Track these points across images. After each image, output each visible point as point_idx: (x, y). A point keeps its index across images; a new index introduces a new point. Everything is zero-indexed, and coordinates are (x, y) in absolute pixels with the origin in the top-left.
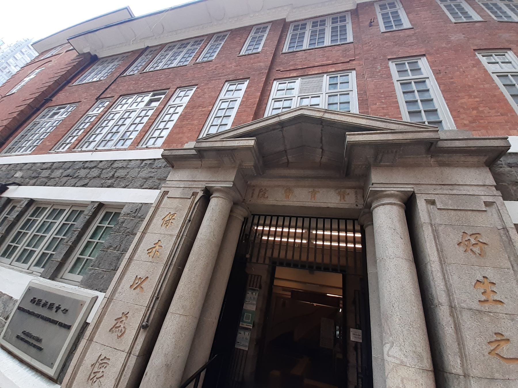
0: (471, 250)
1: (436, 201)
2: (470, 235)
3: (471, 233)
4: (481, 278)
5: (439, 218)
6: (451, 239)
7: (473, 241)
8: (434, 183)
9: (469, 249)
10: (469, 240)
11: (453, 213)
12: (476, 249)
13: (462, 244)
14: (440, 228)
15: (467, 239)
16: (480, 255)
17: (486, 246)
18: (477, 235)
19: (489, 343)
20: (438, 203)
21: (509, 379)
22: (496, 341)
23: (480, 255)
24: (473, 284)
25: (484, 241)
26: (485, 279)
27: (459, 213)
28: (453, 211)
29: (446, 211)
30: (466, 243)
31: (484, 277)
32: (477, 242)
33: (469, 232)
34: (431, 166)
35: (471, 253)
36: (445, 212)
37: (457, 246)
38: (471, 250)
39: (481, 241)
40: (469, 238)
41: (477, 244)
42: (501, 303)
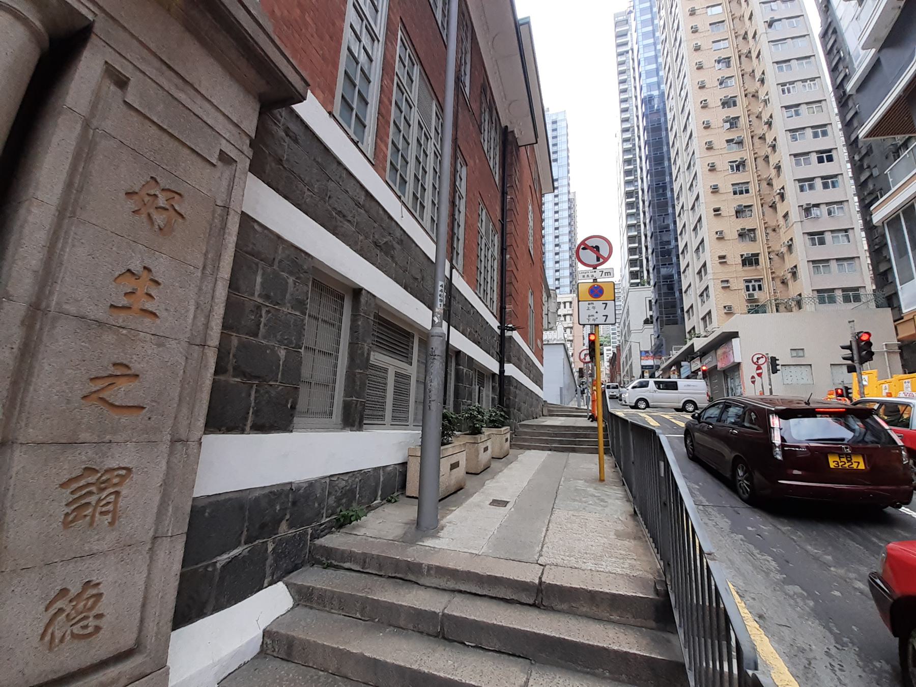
0: (149, 215)
1: (132, 83)
2: (163, 190)
3: (167, 187)
4: (136, 266)
5: (114, 121)
6: (113, 177)
7: (162, 202)
8: (152, 46)
9: (144, 211)
10: (155, 195)
11: (153, 130)
12: (160, 219)
13: (136, 197)
14: (104, 145)
15: (152, 192)
16: (161, 229)
17: (180, 220)
18: (177, 197)
19: (92, 379)
20: (131, 88)
21: (110, 441)
22: (110, 376)
23: (161, 229)
24: (117, 274)
25: (182, 212)
26: (146, 272)
27: (166, 138)
28: (154, 127)
29: (141, 118)
30: (147, 199)
31: (145, 268)
32: (167, 207)
33: (163, 183)
34: (169, 10)
35: (145, 220)
36: (135, 118)
37: (122, 195)
38: (149, 215)
39: (177, 208)
40: (157, 193)
41: (166, 209)
42: (152, 316)
